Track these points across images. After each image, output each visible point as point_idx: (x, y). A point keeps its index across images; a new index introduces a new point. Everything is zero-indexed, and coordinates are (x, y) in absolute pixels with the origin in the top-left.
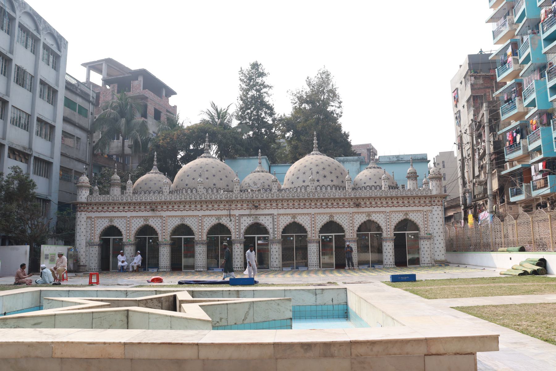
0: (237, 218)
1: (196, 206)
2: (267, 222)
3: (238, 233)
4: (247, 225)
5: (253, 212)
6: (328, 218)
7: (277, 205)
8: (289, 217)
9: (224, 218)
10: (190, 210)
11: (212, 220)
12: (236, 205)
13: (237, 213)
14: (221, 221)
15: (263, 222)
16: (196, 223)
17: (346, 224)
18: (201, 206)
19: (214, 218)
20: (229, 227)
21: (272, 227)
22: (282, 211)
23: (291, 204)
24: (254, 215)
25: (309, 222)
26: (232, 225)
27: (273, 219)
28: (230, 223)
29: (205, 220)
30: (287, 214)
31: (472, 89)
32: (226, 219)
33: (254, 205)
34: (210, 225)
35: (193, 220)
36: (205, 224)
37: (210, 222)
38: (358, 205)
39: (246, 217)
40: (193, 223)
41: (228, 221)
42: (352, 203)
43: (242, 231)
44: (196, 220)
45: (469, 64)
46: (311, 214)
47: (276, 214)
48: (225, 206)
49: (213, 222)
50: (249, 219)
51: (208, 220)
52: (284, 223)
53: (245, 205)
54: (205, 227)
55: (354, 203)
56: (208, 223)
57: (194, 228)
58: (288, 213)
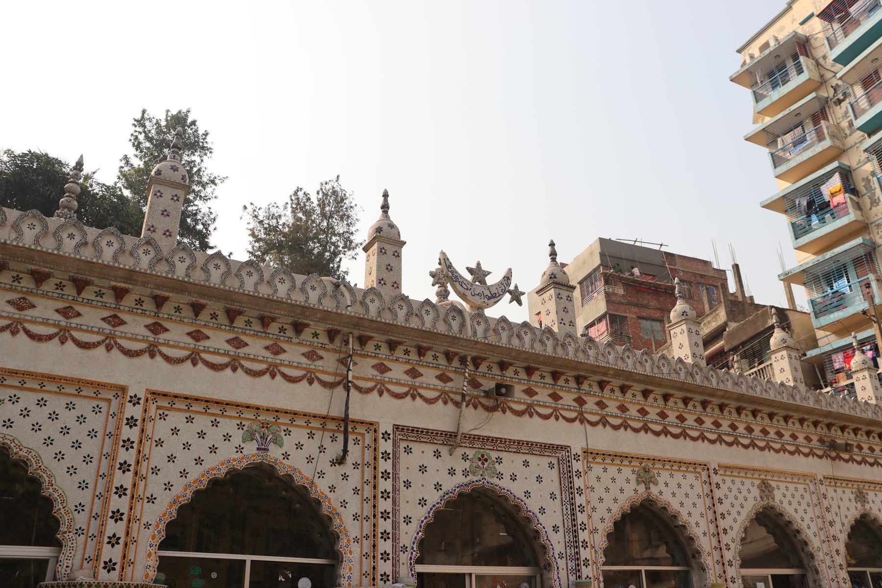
0: (386, 446)
1: (116, 321)
2: (533, 487)
3: (385, 546)
4: (434, 498)
5: (474, 421)
6: (756, 492)
7: (580, 401)
8: (627, 472)
9: (300, 434)
10: (63, 336)
11: (214, 436)
12: (382, 368)
13: (381, 411)
14: (275, 453)
15: (516, 489)
16: (91, 447)
17: (814, 528)
18: (156, 328)
19: (228, 425)
20: (331, 502)
21: (558, 520)
22: (603, 439)
23: (633, 411)
24: (473, 439)
25: (701, 507)
26: (345, 491)
27: (567, 477)
28: (333, 474)
29: (161, 429)
30: (623, 457)
31: (607, 301)
32: (311, 447)
33: (474, 384)
34: (195, 472)
35: (68, 418)
36: (157, 456)
37: (200, 448)
38: (834, 450)
39: (430, 449)
40: (63, 443)
41: (323, 462)
42: (815, 438)
43: (409, 535)
44: (96, 422)
45: (602, 255)
46: (705, 466)
47: (577, 449)
48: (311, 355)
49: (226, 449)
50: (448, 460)
51: (188, 433)
52: (608, 502)
53: (429, 377)
54: (154, 486)
55: (821, 441)
56: (185, 459)
57: (69, 485)
58: (624, 449)
